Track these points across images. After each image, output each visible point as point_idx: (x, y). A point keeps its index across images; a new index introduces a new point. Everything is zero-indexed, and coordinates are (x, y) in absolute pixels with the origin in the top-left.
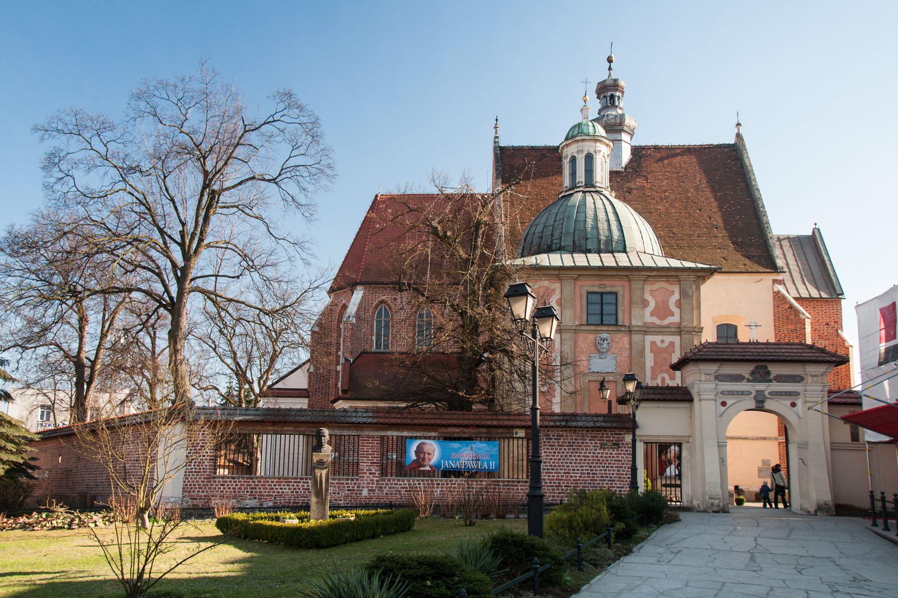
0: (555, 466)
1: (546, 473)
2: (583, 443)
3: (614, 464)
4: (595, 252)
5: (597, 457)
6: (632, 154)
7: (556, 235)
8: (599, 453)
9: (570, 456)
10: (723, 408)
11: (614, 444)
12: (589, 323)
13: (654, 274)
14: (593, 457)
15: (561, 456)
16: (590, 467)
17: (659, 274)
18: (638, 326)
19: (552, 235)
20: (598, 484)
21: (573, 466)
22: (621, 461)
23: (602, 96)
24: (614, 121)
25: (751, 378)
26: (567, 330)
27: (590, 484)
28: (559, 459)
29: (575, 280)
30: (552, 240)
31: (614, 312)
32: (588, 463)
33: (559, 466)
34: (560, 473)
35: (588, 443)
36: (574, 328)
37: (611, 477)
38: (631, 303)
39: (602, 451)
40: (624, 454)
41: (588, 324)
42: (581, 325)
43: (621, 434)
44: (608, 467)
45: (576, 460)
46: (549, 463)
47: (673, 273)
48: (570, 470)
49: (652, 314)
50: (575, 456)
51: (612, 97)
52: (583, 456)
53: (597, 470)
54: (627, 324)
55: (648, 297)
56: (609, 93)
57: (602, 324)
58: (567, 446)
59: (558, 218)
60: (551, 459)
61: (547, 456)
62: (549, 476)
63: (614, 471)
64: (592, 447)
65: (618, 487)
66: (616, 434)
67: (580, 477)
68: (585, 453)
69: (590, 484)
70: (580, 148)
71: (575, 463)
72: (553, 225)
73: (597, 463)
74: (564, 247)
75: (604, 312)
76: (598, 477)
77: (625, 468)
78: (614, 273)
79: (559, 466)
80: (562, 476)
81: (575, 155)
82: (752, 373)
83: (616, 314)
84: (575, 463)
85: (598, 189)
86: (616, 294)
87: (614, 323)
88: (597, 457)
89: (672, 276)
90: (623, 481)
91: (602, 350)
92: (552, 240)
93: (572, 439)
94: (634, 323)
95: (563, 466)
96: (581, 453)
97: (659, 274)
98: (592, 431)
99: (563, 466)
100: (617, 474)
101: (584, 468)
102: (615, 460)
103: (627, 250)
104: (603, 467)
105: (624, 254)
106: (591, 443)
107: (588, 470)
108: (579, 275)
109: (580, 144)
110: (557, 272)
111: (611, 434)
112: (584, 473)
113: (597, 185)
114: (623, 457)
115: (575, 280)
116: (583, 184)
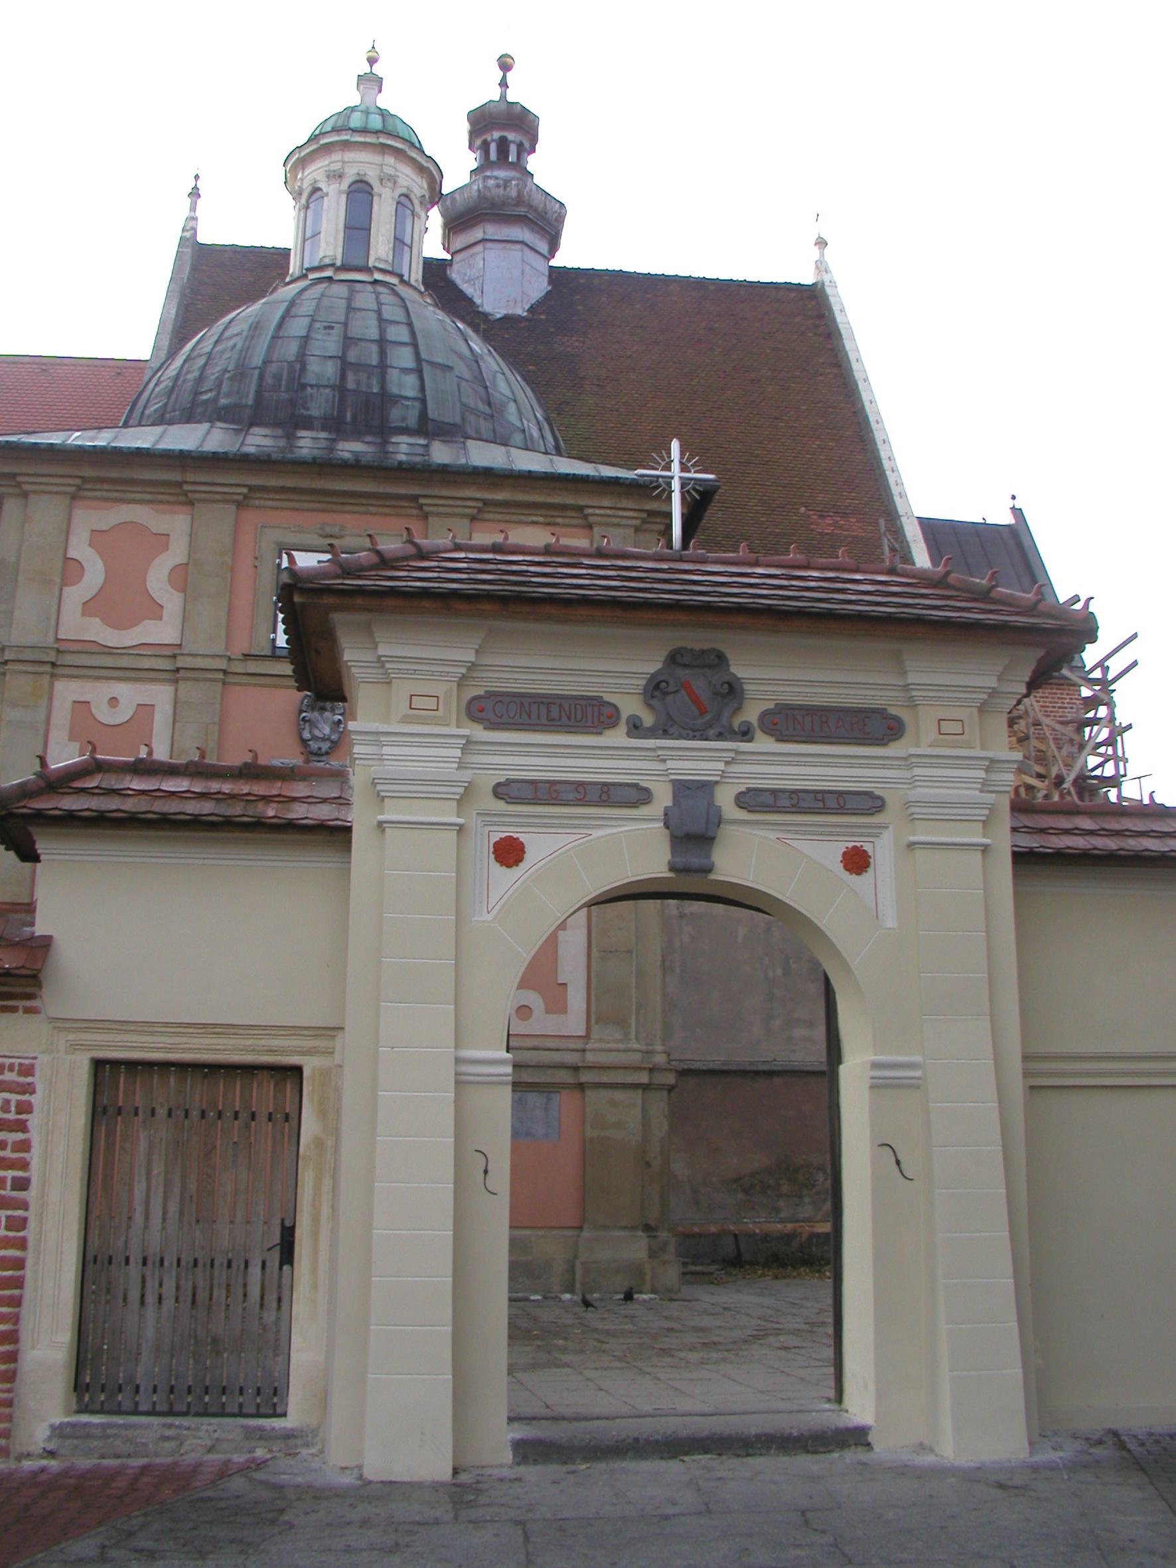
6: (549, 284)
17: (521, 497)
19: (200, 380)
23: (478, 142)
24: (501, 191)
29: (240, 505)
51: (503, 144)
56: (496, 135)
59: (227, 334)
72: (210, 353)
89: (564, 507)
91: (314, 745)
108: (252, 489)
109: (336, 156)
113: (377, 265)
115: (240, 505)
116: (339, 263)
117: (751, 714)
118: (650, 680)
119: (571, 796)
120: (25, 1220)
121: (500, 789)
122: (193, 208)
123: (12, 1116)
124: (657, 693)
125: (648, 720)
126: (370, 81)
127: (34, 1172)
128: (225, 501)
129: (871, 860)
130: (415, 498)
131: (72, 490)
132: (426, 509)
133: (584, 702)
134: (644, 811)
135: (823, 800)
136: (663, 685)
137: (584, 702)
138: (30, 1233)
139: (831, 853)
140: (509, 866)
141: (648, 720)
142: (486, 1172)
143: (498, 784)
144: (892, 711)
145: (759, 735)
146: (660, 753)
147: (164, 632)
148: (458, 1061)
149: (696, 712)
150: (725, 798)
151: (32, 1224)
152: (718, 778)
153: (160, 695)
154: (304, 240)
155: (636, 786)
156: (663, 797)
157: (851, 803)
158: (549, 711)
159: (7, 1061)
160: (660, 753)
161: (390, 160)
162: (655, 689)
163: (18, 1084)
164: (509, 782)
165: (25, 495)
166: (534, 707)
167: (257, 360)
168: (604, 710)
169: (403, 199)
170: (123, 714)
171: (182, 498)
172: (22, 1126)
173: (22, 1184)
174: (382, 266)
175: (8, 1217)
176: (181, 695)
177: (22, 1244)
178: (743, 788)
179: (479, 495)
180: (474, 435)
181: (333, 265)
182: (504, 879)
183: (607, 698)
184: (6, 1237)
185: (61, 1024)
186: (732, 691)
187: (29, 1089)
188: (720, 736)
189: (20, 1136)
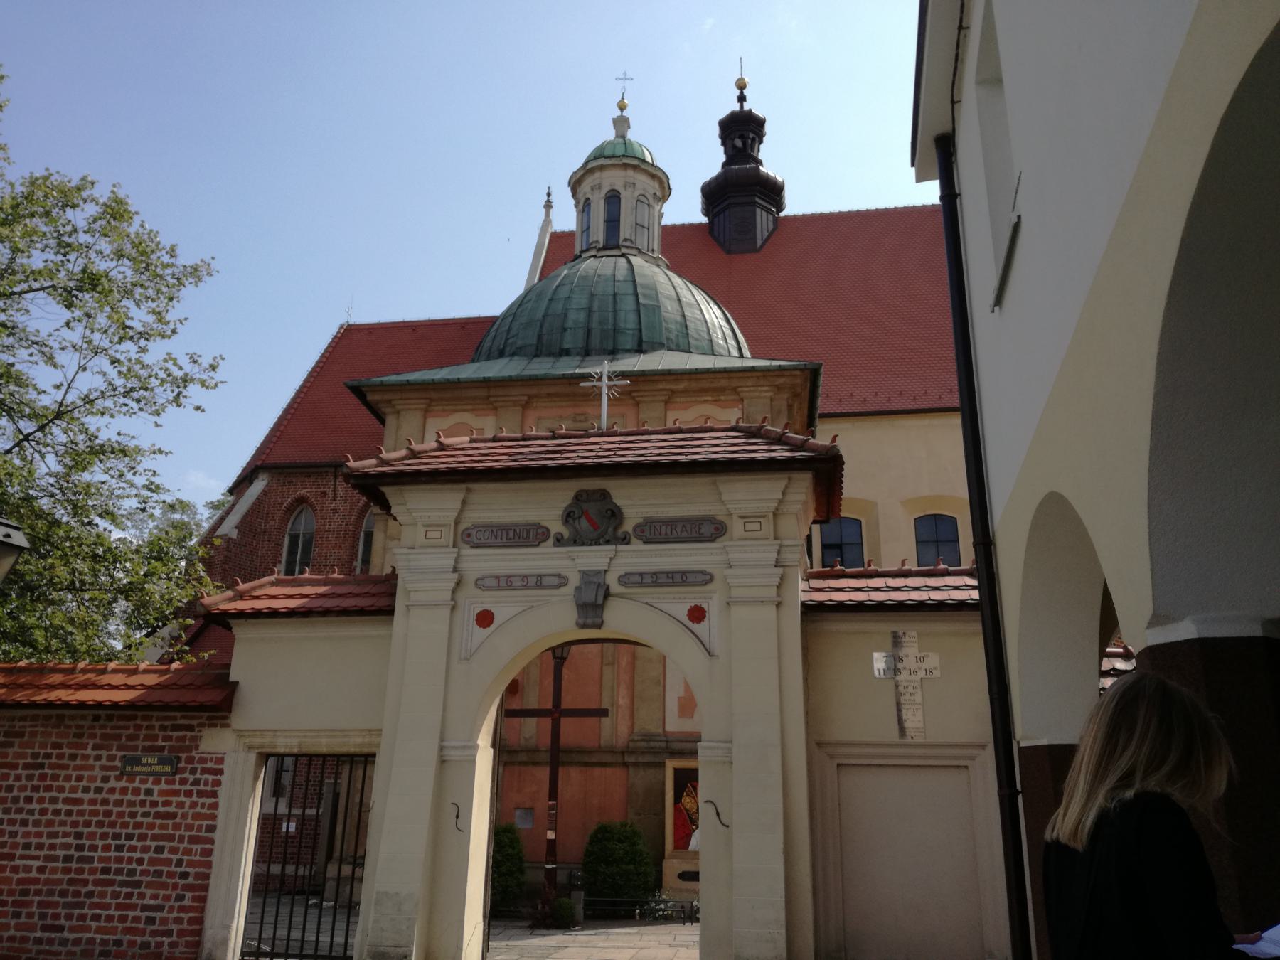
2: (73, 757)
3: (151, 826)
4: (578, 354)
7: (513, 332)
8: (112, 791)
9: (29, 800)
10: (480, 633)
11: (162, 762)
14: (93, 802)
16: (79, 836)
19: (509, 331)
20: (90, 894)
21: (27, 835)
22: (174, 816)
27: (63, 894)
32: (75, 824)
35: (86, 757)
37: (132, 872)
39: (123, 784)
40: (189, 794)
44: (130, 837)
47: (723, 383)
48: (15, 846)
52: (66, 801)
53: (93, 848)
58: (26, 766)
63: (145, 849)
65: (145, 908)
66: (176, 728)
67: (41, 870)
68: (74, 790)
69: (63, 894)
70: (597, 182)
71: (36, 823)
73: (100, 824)
74: (520, 348)
76: (92, 871)
77: (181, 839)
81: (588, 196)
90: (164, 886)
92: (507, 339)
93: (43, 746)
96: (61, 789)
97: (694, 385)
98: (110, 718)
100: (152, 862)
102: (158, 815)
103: (644, 347)
104: (117, 836)
106: (98, 758)
107: (66, 846)
108: (530, 397)
109: (597, 174)
110: (483, 393)
111: (163, 728)
112: (56, 859)
113: (625, 244)
114: (180, 805)
116: (601, 245)
117: (628, 527)
118: (564, 511)
119: (519, 584)
120: (212, 850)
121: (479, 582)
122: (547, 214)
123: (209, 788)
124: (570, 519)
125: (566, 534)
126: (621, 124)
127: (220, 823)
129: (707, 614)
131: (423, 406)
132: (637, 399)
133: (528, 528)
134: (563, 590)
135: (673, 578)
136: (572, 514)
137: (528, 528)
138: (215, 858)
139: (682, 611)
140: (484, 627)
141: (566, 534)
142: (457, 817)
143: (478, 580)
144: (719, 518)
145: (634, 540)
146: (570, 554)
148: (442, 748)
149: (592, 529)
150: (612, 580)
151: (216, 853)
152: (606, 568)
154: (582, 232)
155: (559, 576)
156: (575, 580)
157: (691, 578)
158: (508, 534)
159: (209, 756)
160: (570, 554)
161: (630, 172)
162: (568, 517)
163: (215, 769)
164: (483, 579)
165: (398, 412)
166: (499, 533)
167: (539, 315)
168: (540, 531)
169: (642, 198)
171: (491, 406)
172: (214, 794)
173: (212, 829)
174: (628, 244)
175: (201, 849)
178: (623, 573)
179: (668, 387)
180: (674, 348)
181: (595, 247)
183: (543, 523)
184: (199, 860)
185: (240, 733)
186: (615, 515)
187: (221, 772)
188: (608, 542)
189: (212, 800)
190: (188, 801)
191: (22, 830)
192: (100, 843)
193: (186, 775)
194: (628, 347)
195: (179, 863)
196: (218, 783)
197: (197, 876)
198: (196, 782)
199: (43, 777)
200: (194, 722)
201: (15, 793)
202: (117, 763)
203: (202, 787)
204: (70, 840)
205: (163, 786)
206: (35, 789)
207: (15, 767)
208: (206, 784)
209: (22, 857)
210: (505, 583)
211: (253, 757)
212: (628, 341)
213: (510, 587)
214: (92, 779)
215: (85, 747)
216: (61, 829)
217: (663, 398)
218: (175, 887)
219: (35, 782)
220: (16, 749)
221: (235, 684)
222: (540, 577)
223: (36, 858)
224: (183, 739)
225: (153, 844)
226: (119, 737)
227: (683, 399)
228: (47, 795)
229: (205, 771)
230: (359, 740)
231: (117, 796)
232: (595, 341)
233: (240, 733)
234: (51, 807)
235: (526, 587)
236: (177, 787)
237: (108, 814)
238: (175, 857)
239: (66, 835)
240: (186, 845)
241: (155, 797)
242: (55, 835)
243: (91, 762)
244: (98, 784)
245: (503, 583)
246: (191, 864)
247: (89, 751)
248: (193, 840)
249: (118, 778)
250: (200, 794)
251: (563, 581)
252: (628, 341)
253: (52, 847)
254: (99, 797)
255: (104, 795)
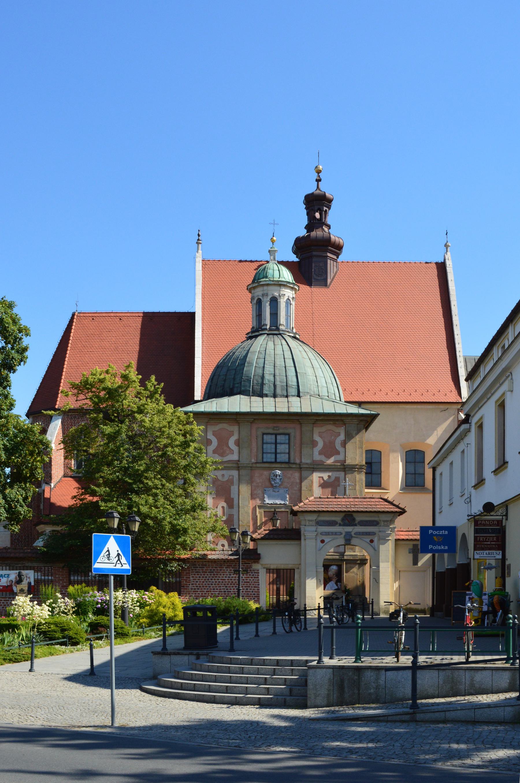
0: (200, 587)
1: (194, 591)
2: (221, 570)
5: (231, 580)
8: (232, 577)
9: (211, 579)
12: (265, 460)
13: (320, 418)
14: (228, 580)
15: (205, 580)
16: (226, 587)
17: (326, 418)
18: (307, 464)
21: (213, 587)
22: (249, 582)
25: (342, 523)
26: (245, 467)
28: (203, 582)
30: (234, 384)
31: (287, 451)
32: (225, 584)
33: (203, 587)
34: (204, 591)
35: (224, 570)
36: (251, 465)
38: (301, 444)
40: (252, 578)
41: (263, 462)
42: (256, 463)
43: (249, 563)
45: (216, 582)
46: (196, 584)
48: (211, 589)
49: (320, 453)
50: (215, 579)
52: (221, 579)
53: (231, 589)
54: (298, 461)
55: (317, 438)
57: (276, 462)
58: (209, 572)
60: (197, 582)
61: (194, 579)
62: (196, 594)
64: (228, 573)
68: (223, 577)
71: (215, 584)
73: (231, 584)
75: (278, 451)
77: (252, 587)
78: (286, 418)
79: (203, 587)
80: (205, 594)
82: (343, 520)
83: (289, 453)
84: (215, 584)
85: (281, 332)
86: (289, 435)
87: (287, 460)
88: (231, 580)
90: (250, 596)
93: (212, 568)
94: (303, 461)
95: (206, 587)
96: (219, 577)
97: (326, 418)
99: (206, 587)
100: (246, 592)
101: (222, 588)
102: (245, 582)
103: (301, 395)
105: (298, 398)
107: (224, 589)
112: (222, 592)
114: (250, 580)
128: (248, 422)
130: (298, 420)
147: (235, 457)
153: (235, 473)
170: (225, 479)
173: (259, 585)
176: (240, 473)
177: (259, 592)
182: (322, 545)
185: (262, 565)
187: (259, 573)
190: (252, 579)
191: (211, 586)
192: (232, 588)
193: (250, 574)
194: (293, 394)
195: (252, 592)
196: (258, 575)
197: (257, 594)
198: (253, 575)
199: (214, 575)
200: (250, 562)
201: (208, 578)
202: (232, 571)
203: (255, 576)
204: (224, 588)
205: (245, 576)
206: (213, 577)
207: (206, 572)
208: (256, 575)
209: (213, 591)
210: (327, 534)
211: (265, 570)
212: (293, 391)
213: (329, 535)
214: (227, 575)
215: (223, 568)
216: (221, 586)
217: (312, 422)
218: (252, 596)
219: (212, 576)
220: (205, 568)
221: (259, 554)
222: (336, 533)
223: (217, 592)
224: (248, 566)
225: (245, 588)
226: (231, 566)
227: (320, 423)
228: (216, 578)
229: (254, 573)
230: (291, 566)
231: (234, 578)
232: (279, 391)
233: (262, 565)
234: (218, 581)
235: (332, 535)
236: (248, 576)
237: (232, 582)
238: (251, 591)
239: (223, 587)
240: (253, 588)
241: (243, 578)
242: (220, 587)
243: (226, 571)
244: (229, 576)
245: (327, 534)
246: (255, 592)
247: (224, 569)
248: (254, 587)
249: (234, 574)
250: (255, 578)
251: (341, 534)
252: (293, 391)
253: (220, 589)
254: (230, 579)
255: (231, 578)
